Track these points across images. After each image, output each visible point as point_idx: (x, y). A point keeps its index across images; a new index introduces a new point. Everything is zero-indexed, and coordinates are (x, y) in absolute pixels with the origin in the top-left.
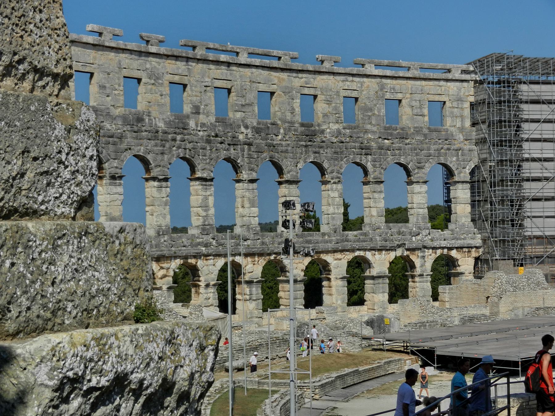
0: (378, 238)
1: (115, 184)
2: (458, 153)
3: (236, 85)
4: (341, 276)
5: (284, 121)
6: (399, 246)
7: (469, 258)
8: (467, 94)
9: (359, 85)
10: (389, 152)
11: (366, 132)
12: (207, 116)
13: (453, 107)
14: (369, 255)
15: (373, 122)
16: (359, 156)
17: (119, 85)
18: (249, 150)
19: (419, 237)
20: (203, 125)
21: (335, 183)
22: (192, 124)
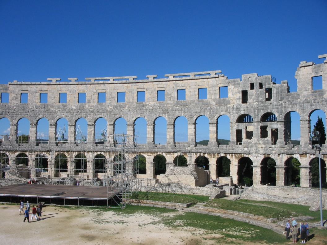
0: (169, 147)
1: (52, 127)
2: (210, 111)
3: (108, 91)
4: (150, 162)
5: (129, 103)
6: (179, 151)
7: (214, 158)
8: (218, 83)
9: (165, 85)
10: (176, 112)
11: (168, 104)
12: (94, 103)
13: (211, 90)
14: (164, 154)
15: (171, 100)
16: (162, 114)
17: (57, 96)
18: (110, 114)
19: (189, 148)
20: (92, 106)
21: (149, 125)
22: (87, 106)
